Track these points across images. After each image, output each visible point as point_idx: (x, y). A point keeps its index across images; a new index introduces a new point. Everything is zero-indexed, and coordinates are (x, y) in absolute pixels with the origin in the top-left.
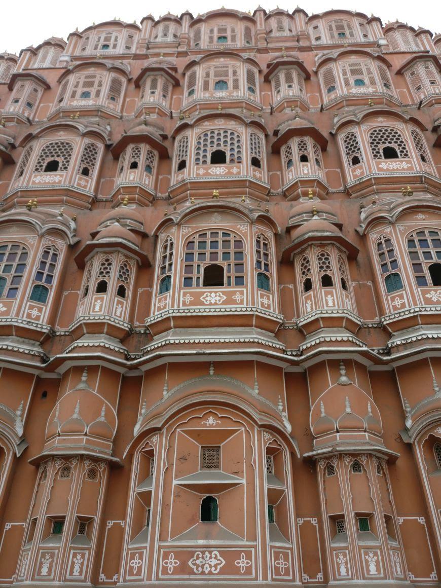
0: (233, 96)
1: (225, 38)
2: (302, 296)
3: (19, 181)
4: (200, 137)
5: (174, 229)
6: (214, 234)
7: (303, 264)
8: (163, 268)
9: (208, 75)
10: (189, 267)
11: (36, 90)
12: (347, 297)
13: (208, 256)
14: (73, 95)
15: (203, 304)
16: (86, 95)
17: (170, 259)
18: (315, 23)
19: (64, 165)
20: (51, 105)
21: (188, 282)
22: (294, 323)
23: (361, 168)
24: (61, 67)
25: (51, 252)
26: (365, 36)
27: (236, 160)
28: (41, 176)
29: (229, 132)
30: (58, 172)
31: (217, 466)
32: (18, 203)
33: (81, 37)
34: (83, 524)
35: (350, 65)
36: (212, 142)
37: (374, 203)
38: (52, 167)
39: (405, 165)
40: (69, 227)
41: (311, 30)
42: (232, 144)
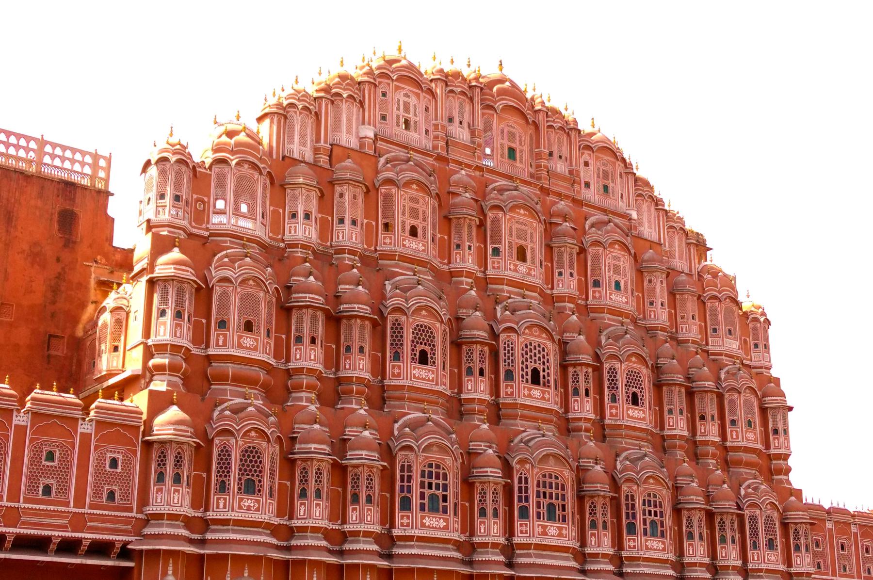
0: (531, 275)
2: (589, 532)
3: (399, 367)
5: (528, 466)
7: (590, 507)
9: (511, 235)
15: (547, 534)
16: (414, 232)
17: (526, 492)
18: (586, 156)
19: (432, 358)
23: (617, 408)
28: (419, 368)
33: (375, 86)
36: (531, 358)
38: (423, 359)
42: (544, 364)
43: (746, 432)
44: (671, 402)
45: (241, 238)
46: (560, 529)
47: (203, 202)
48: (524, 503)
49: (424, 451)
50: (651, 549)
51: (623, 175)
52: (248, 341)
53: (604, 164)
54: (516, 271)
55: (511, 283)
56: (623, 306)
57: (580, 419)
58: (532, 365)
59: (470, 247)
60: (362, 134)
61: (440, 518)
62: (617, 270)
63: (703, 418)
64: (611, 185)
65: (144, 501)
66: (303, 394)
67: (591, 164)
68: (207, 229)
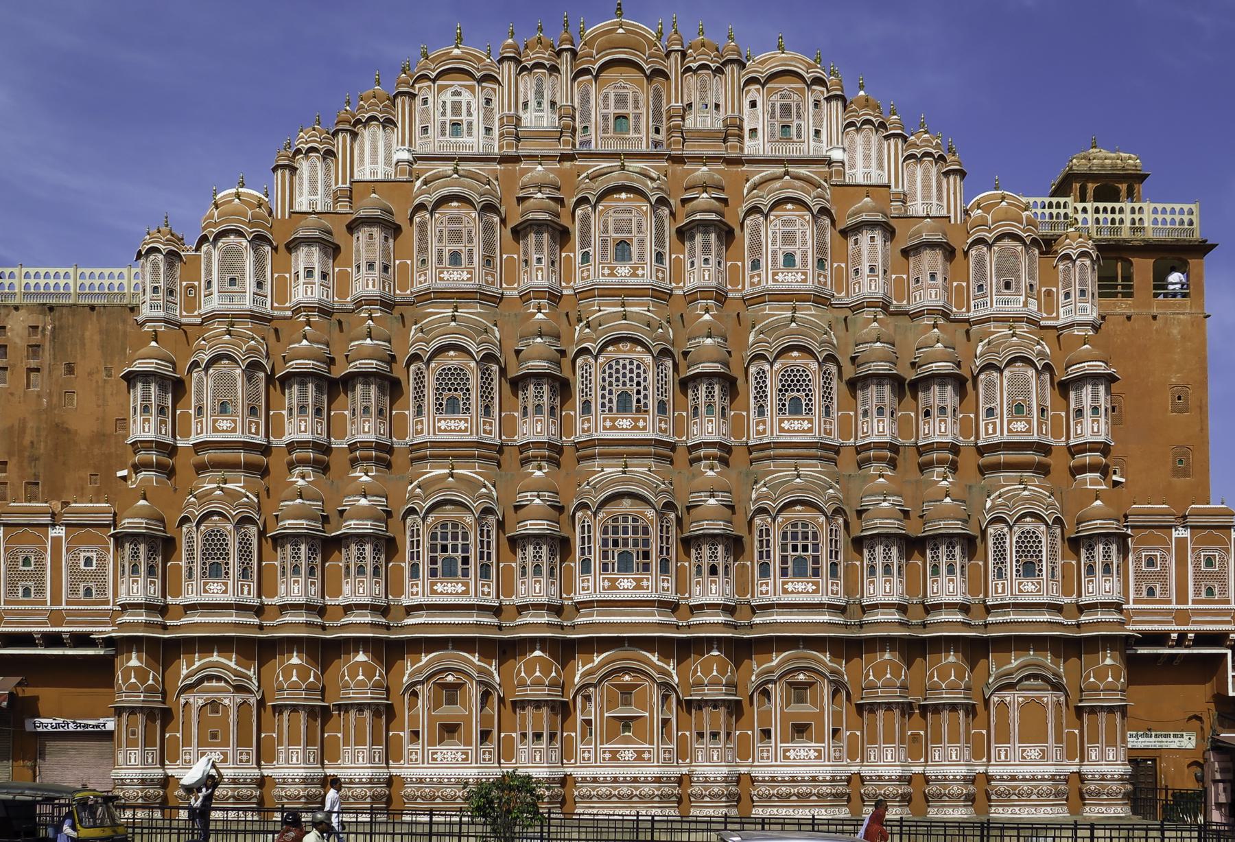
0: (637, 276)
1: (625, 117)
3: (422, 422)
4: (604, 372)
6: (625, 519)
8: (583, 549)
10: (605, 555)
11: (386, 239)
13: (620, 541)
16: (455, 258)
18: (754, 92)
21: (605, 568)
24: (405, 178)
26: (817, 132)
29: (635, 363)
30: (461, 416)
31: (630, 704)
32: (432, 456)
34: (552, 737)
35: (785, 223)
36: (617, 380)
37: (765, 485)
38: (452, 407)
39: (806, 425)
40: (492, 499)
41: (746, 104)
42: (638, 384)
43: (1009, 423)
44: (865, 402)
45: (226, 316)
46: (638, 581)
47: (193, 287)
48: (587, 555)
49: (431, 509)
50: (792, 592)
52: (224, 424)
53: (783, 97)
54: (612, 275)
56: (795, 286)
57: (698, 446)
58: (617, 389)
59: (539, 260)
60: (394, 161)
62: (788, 238)
63: (927, 414)
65: (115, 594)
66: (297, 471)
67: (759, 104)
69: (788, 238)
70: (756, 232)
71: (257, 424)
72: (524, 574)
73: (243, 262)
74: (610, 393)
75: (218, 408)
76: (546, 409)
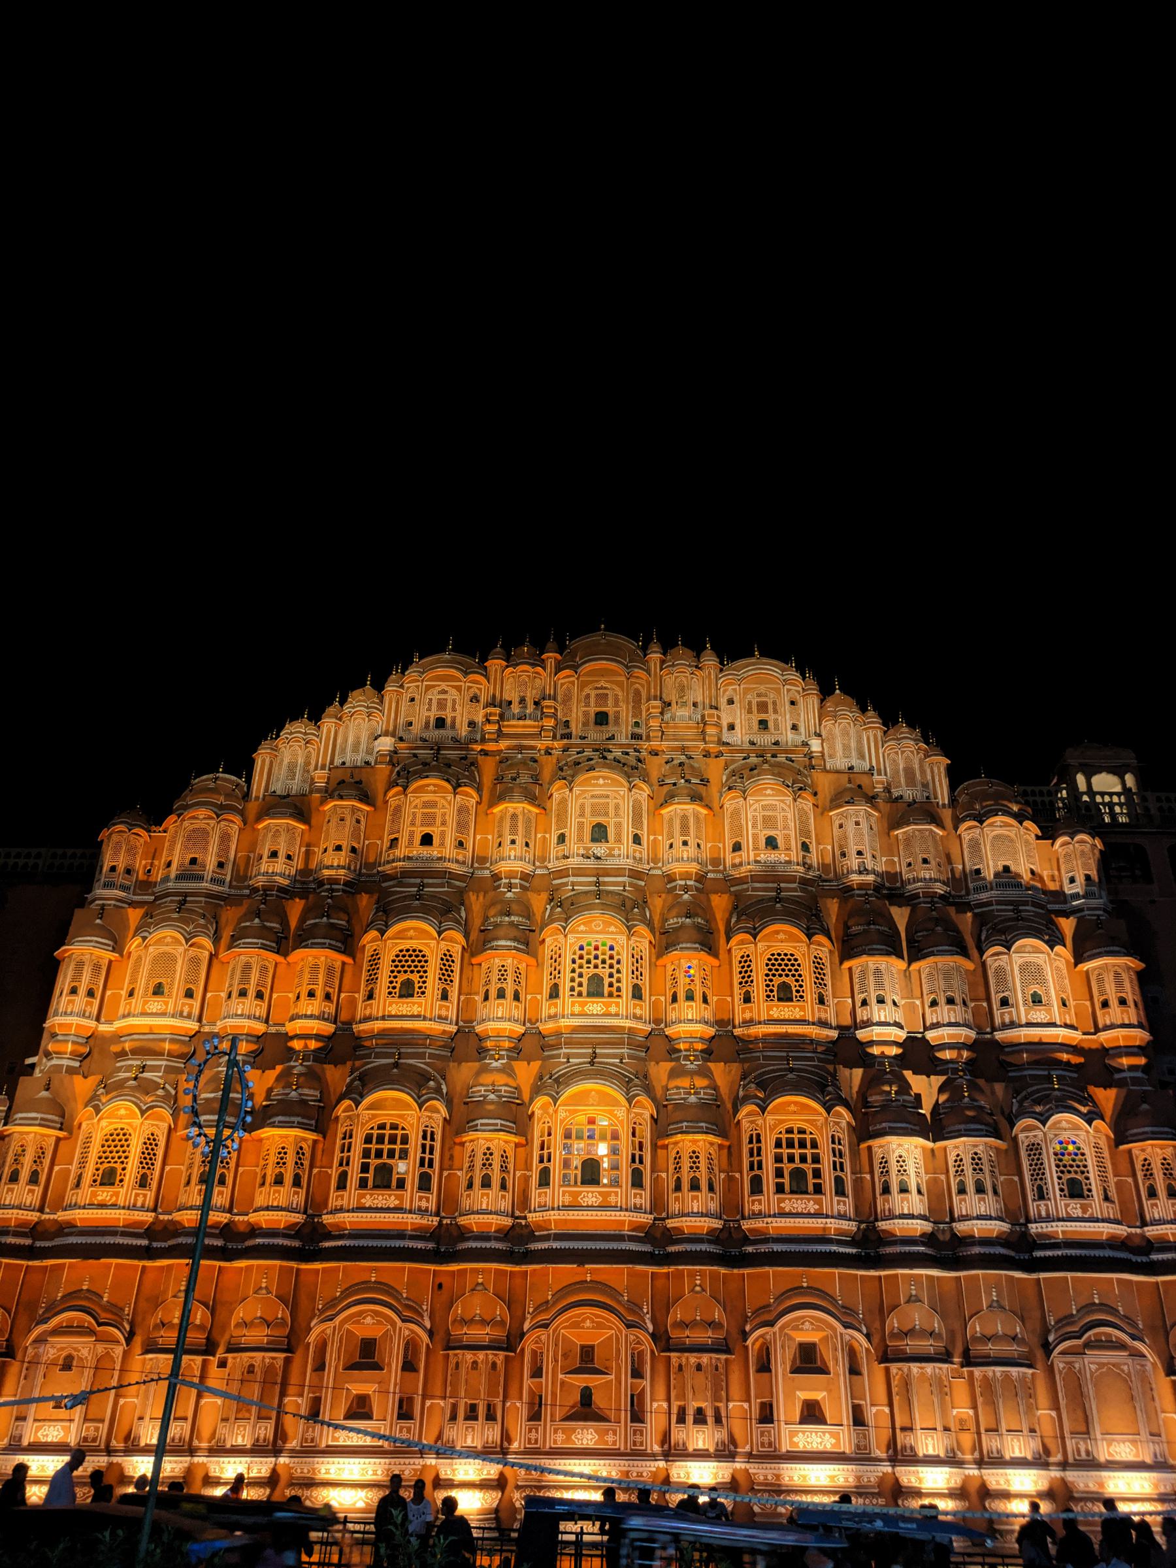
9: (582, 815)
12: (712, 1199)
14: (411, 842)
20: (379, 842)
22: (663, 1219)
25: (429, 1130)
26: (795, 727)
27: (615, 994)
28: (397, 1003)
30: (415, 999)
38: (407, 990)
39: (798, 1014)
42: (611, 966)
46: (605, 1195)
51: (800, 701)
52: (155, 1005)
53: (759, 695)
55: (579, 872)
58: (588, 972)
59: (513, 842)
61: (390, 1196)
62: (769, 822)
64: (771, 717)
68: (153, 894)
69: (769, 822)
70: (736, 813)
71: (191, 1006)
72: (470, 1186)
73: (207, 843)
74: (581, 975)
75: (151, 990)
76: (509, 993)
